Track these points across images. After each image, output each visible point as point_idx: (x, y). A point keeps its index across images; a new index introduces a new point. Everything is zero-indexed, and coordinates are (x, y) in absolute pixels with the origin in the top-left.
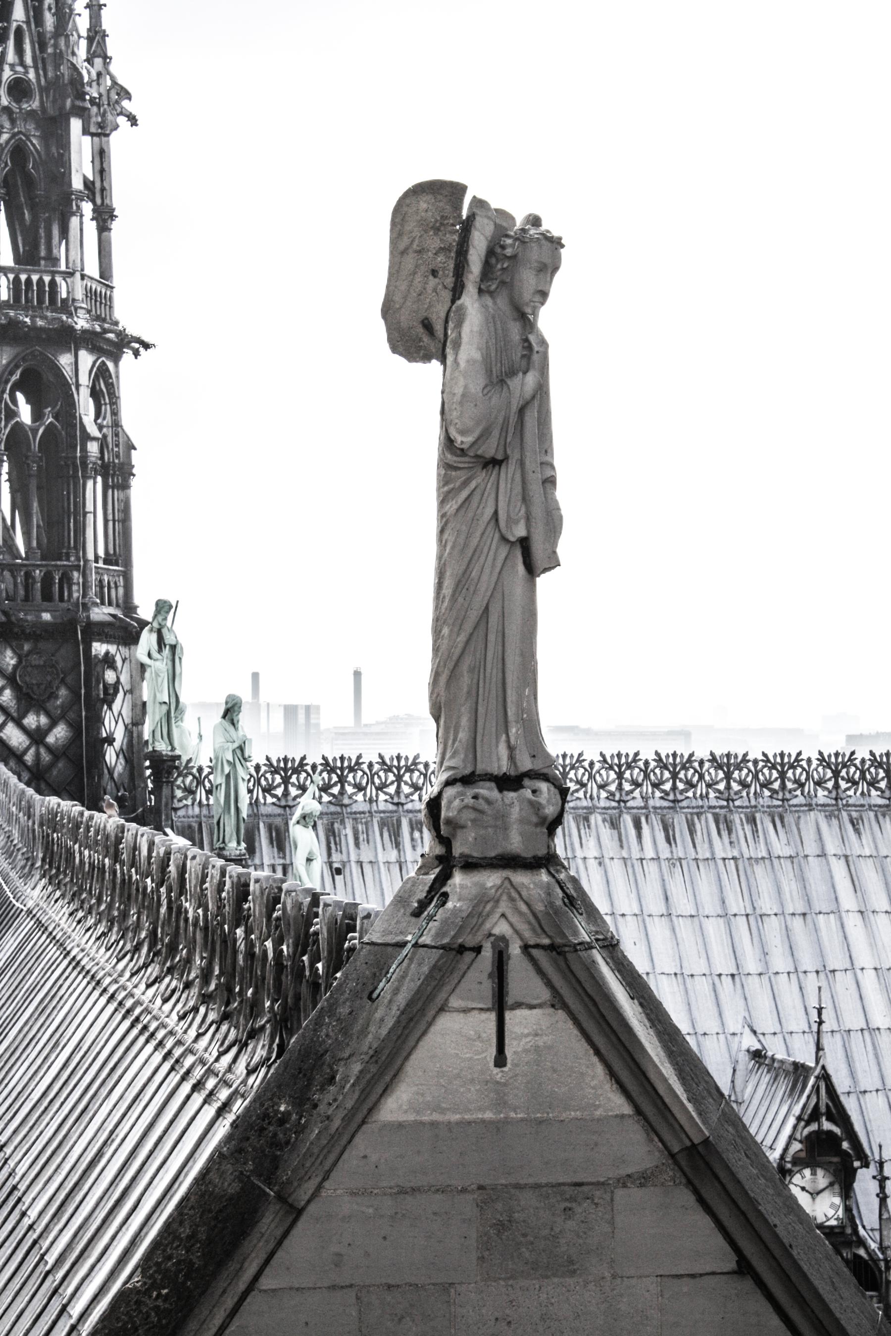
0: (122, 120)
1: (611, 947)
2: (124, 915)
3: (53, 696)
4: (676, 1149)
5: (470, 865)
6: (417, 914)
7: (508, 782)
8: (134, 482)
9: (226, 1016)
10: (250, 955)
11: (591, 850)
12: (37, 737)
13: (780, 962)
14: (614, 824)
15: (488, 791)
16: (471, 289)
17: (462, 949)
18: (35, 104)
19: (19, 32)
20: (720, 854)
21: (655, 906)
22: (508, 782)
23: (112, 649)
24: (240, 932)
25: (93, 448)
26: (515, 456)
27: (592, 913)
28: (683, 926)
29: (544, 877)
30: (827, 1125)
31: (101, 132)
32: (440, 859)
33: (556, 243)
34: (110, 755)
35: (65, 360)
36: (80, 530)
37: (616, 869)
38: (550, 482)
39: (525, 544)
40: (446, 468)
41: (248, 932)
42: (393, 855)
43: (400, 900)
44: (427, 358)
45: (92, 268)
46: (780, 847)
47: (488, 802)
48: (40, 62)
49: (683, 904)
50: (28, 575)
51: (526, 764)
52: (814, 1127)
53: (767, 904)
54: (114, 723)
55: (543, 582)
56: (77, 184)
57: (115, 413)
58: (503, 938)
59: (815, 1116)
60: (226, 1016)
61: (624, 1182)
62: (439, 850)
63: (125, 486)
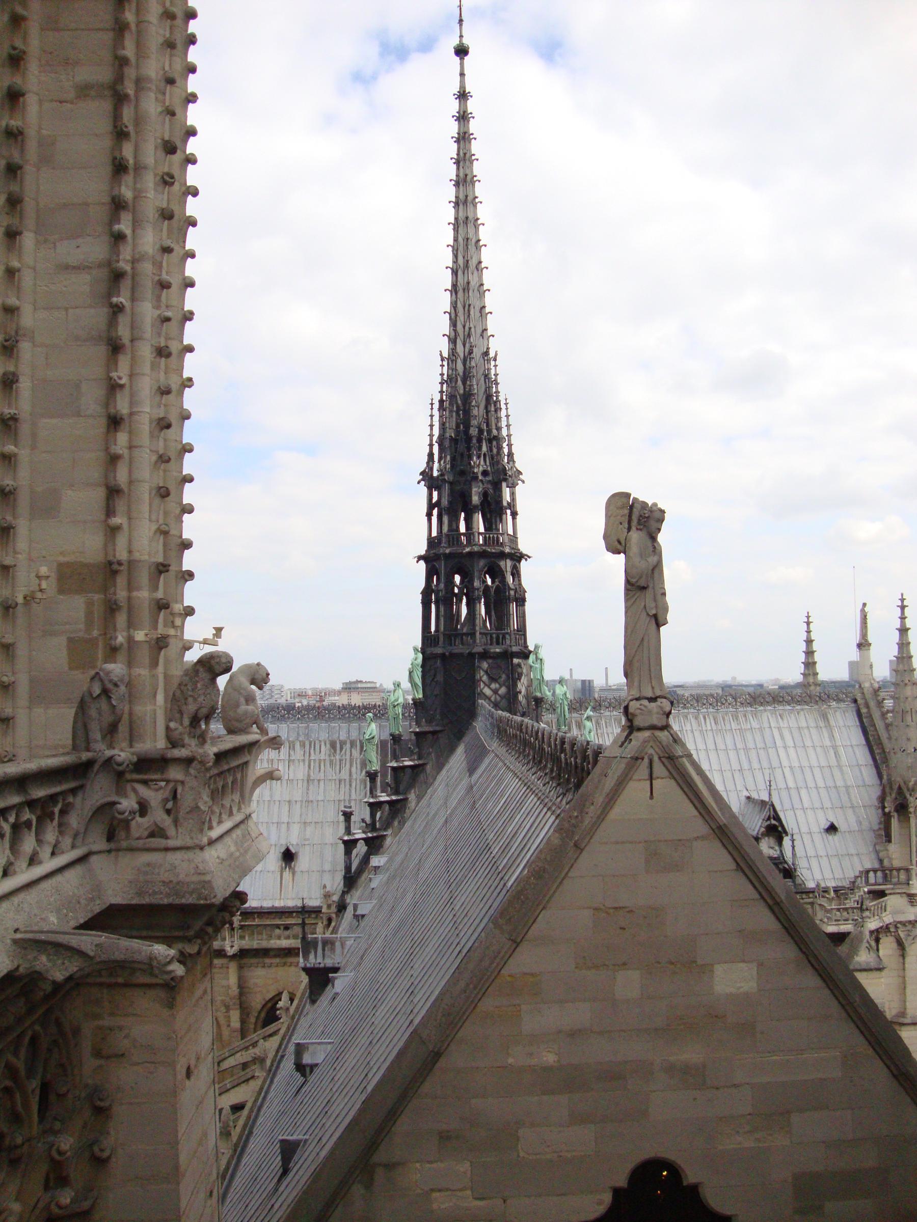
0: (519, 482)
1: (689, 756)
2: (524, 750)
3: (500, 677)
4: (714, 827)
5: (639, 729)
6: (621, 746)
7: (652, 700)
8: (526, 604)
9: (559, 785)
10: (566, 763)
12: (495, 692)
13: (755, 765)
14: (696, 718)
15: (645, 702)
16: (634, 528)
17: (637, 759)
18: (490, 478)
19: (485, 455)
20: (733, 727)
21: (711, 746)
22: (652, 700)
23: (520, 661)
24: (563, 755)
25: (512, 593)
26: (651, 585)
27: (683, 745)
29: (666, 733)
30: (773, 822)
31: (513, 486)
32: (629, 727)
33: (663, 512)
34: (520, 697)
35: (502, 564)
36: (508, 621)
37: (697, 734)
38: (664, 594)
39: (655, 616)
40: (627, 590)
41: (566, 755)
43: (615, 741)
44: (619, 553)
45: (511, 532)
47: (645, 707)
48: (492, 465)
49: (721, 746)
50: (491, 637)
51: (658, 693)
52: (768, 822)
54: (522, 686)
55: (662, 629)
56: (505, 504)
57: (520, 581)
58: (652, 755)
59: (769, 819)
60: (559, 785)
61: (697, 838)
62: (629, 724)
63: (524, 605)
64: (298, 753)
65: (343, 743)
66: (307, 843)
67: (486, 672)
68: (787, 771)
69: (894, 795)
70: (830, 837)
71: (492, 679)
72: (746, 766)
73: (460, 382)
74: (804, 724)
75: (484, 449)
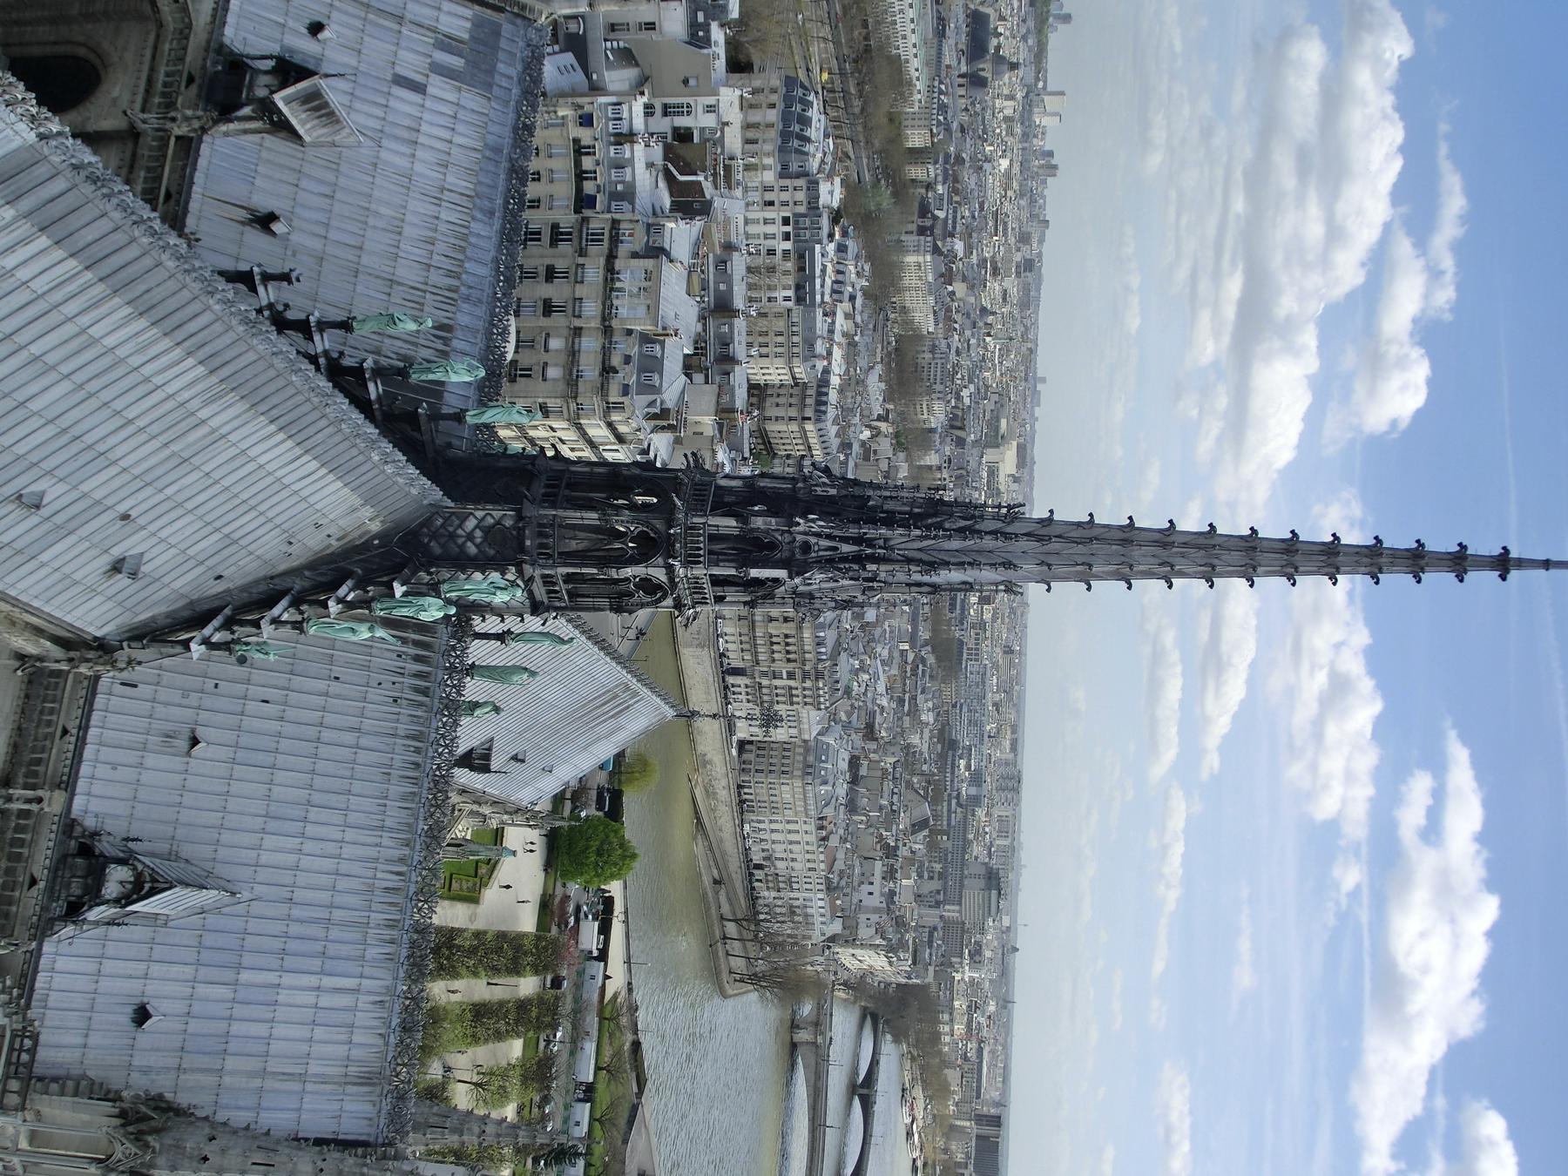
11: (385, 842)
12: (470, 537)
13: (295, 929)
14: (402, 860)
20: (373, 915)
21: (345, 867)
28: (326, 880)
30: (147, 886)
37: (372, 852)
42: (402, 733)
46: (373, 952)
49: (343, 884)
53: (335, 933)
59: (154, 880)
63: (611, 610)
64: (436, 278)
65: (446, 341)
66: (289, 253)
67: (498, 523)
68: (272, 978)
69: (143, 1109)
70: (130, 1010)
71: (488, 531)
72: (297, 912)
73: (963, 523)
74: (357, 1038)
75: (846, 548)
